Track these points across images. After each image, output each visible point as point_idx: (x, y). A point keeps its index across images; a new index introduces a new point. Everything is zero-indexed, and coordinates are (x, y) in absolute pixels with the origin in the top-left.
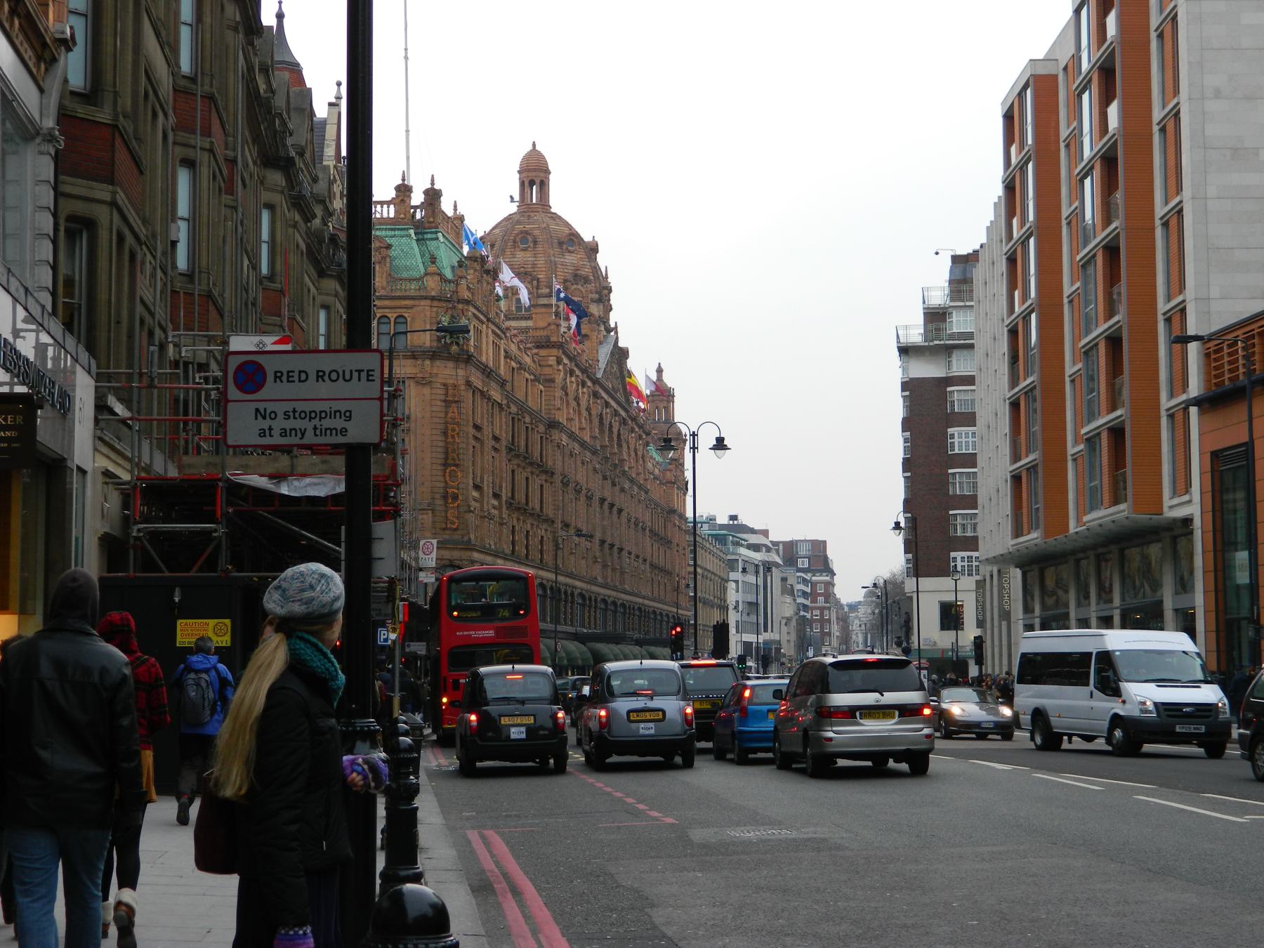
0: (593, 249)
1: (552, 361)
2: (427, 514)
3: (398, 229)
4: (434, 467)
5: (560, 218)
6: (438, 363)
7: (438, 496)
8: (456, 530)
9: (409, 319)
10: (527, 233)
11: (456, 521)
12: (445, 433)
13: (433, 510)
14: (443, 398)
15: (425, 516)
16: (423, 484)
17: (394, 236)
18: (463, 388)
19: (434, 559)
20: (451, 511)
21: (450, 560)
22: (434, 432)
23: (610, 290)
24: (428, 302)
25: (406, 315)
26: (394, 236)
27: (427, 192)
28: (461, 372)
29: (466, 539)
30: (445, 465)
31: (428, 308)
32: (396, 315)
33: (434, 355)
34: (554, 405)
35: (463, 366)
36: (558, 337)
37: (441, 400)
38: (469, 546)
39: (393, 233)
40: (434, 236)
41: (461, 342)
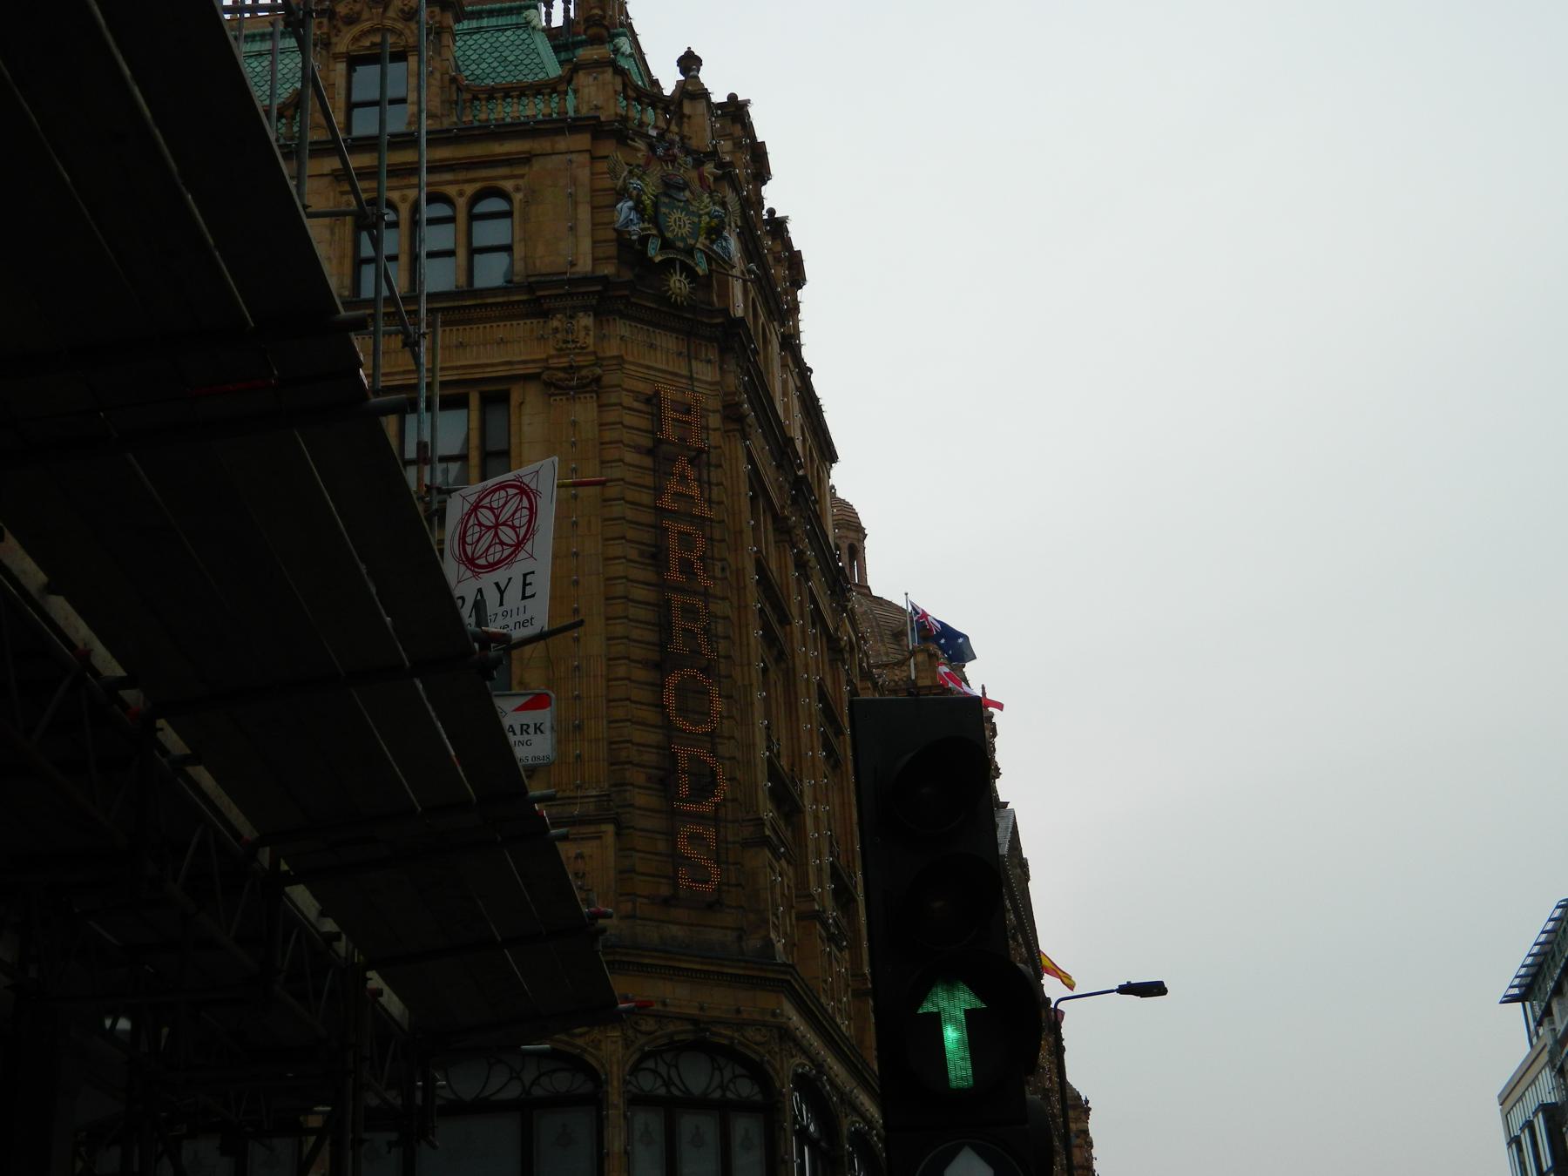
2: (598, 837)
3: (491, 13)
4: (621, 671)
5: (890, 603)
8: (713, 906)
11: (714, 870)
12: (656, 557)
14: (646, 442)
15: (588, 848)
16: (579, 728)
17: (478, 30)
18: (714, 421)
19: (542, 585)
20: (687, 829)
21: (694, 1021)
24: (583, 141)
25: (508, 185)
26: (478, 30)
28: (706, 372)
29: (753, 943)
30: (662, 664)
31: (587, 156)
37: (638, 449)
41: (702, 268)
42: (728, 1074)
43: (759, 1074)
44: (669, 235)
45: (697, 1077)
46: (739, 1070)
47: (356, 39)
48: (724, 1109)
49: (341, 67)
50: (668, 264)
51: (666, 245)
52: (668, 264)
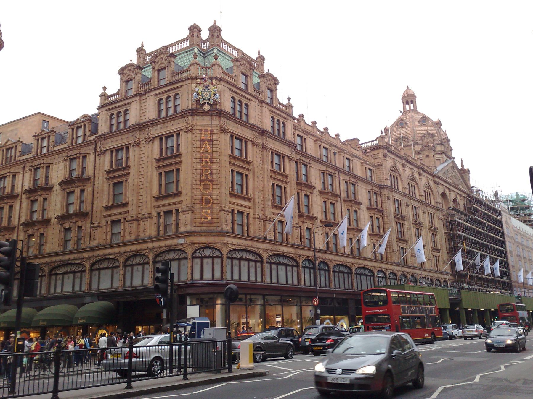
0: (438, 124)
1: (381, 155)
3: (189, 51)
4: (195, 183)
6: (198, 117)
7: (198, 201)
9: (180, 94)
10: (402, 120)
12: (201, 161)
13: (193, 212)
17: (188, 55)
22: (195, 161)
23: (448, 141)
25: (179, 92)
26: (188, 55)
27: (210, 30)
32: (175, 93)
33: (192, 112)
34: (383, 177)
35: (217, 118)
36: (383, 143)
38: (222, 234)
39: (186, 54)
40: (212, 52)
42: (214, 252)
43: (220, 251)
44: (204, 98)
45: (207, 252)
46: (216, 251)
47: (158, 66)
48: (213, 258)
49: (156, 72)
50: (204, 104)
51: (204, 100)
52: (204, 104)
